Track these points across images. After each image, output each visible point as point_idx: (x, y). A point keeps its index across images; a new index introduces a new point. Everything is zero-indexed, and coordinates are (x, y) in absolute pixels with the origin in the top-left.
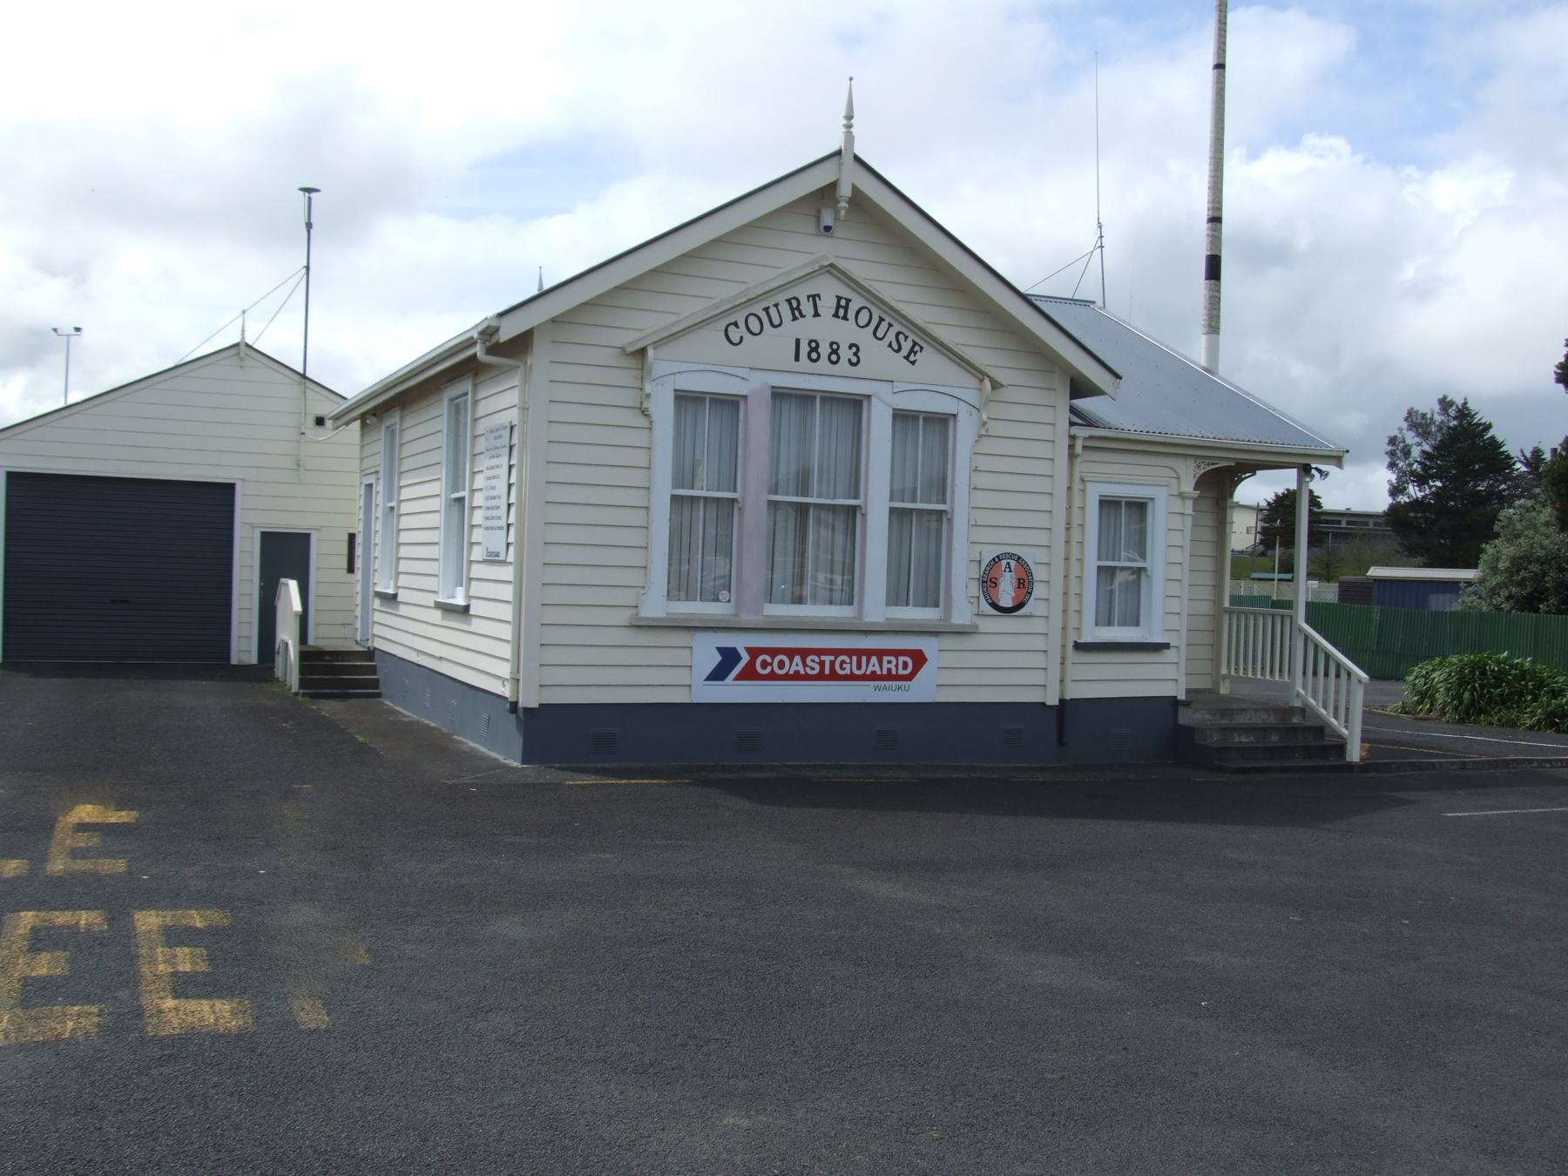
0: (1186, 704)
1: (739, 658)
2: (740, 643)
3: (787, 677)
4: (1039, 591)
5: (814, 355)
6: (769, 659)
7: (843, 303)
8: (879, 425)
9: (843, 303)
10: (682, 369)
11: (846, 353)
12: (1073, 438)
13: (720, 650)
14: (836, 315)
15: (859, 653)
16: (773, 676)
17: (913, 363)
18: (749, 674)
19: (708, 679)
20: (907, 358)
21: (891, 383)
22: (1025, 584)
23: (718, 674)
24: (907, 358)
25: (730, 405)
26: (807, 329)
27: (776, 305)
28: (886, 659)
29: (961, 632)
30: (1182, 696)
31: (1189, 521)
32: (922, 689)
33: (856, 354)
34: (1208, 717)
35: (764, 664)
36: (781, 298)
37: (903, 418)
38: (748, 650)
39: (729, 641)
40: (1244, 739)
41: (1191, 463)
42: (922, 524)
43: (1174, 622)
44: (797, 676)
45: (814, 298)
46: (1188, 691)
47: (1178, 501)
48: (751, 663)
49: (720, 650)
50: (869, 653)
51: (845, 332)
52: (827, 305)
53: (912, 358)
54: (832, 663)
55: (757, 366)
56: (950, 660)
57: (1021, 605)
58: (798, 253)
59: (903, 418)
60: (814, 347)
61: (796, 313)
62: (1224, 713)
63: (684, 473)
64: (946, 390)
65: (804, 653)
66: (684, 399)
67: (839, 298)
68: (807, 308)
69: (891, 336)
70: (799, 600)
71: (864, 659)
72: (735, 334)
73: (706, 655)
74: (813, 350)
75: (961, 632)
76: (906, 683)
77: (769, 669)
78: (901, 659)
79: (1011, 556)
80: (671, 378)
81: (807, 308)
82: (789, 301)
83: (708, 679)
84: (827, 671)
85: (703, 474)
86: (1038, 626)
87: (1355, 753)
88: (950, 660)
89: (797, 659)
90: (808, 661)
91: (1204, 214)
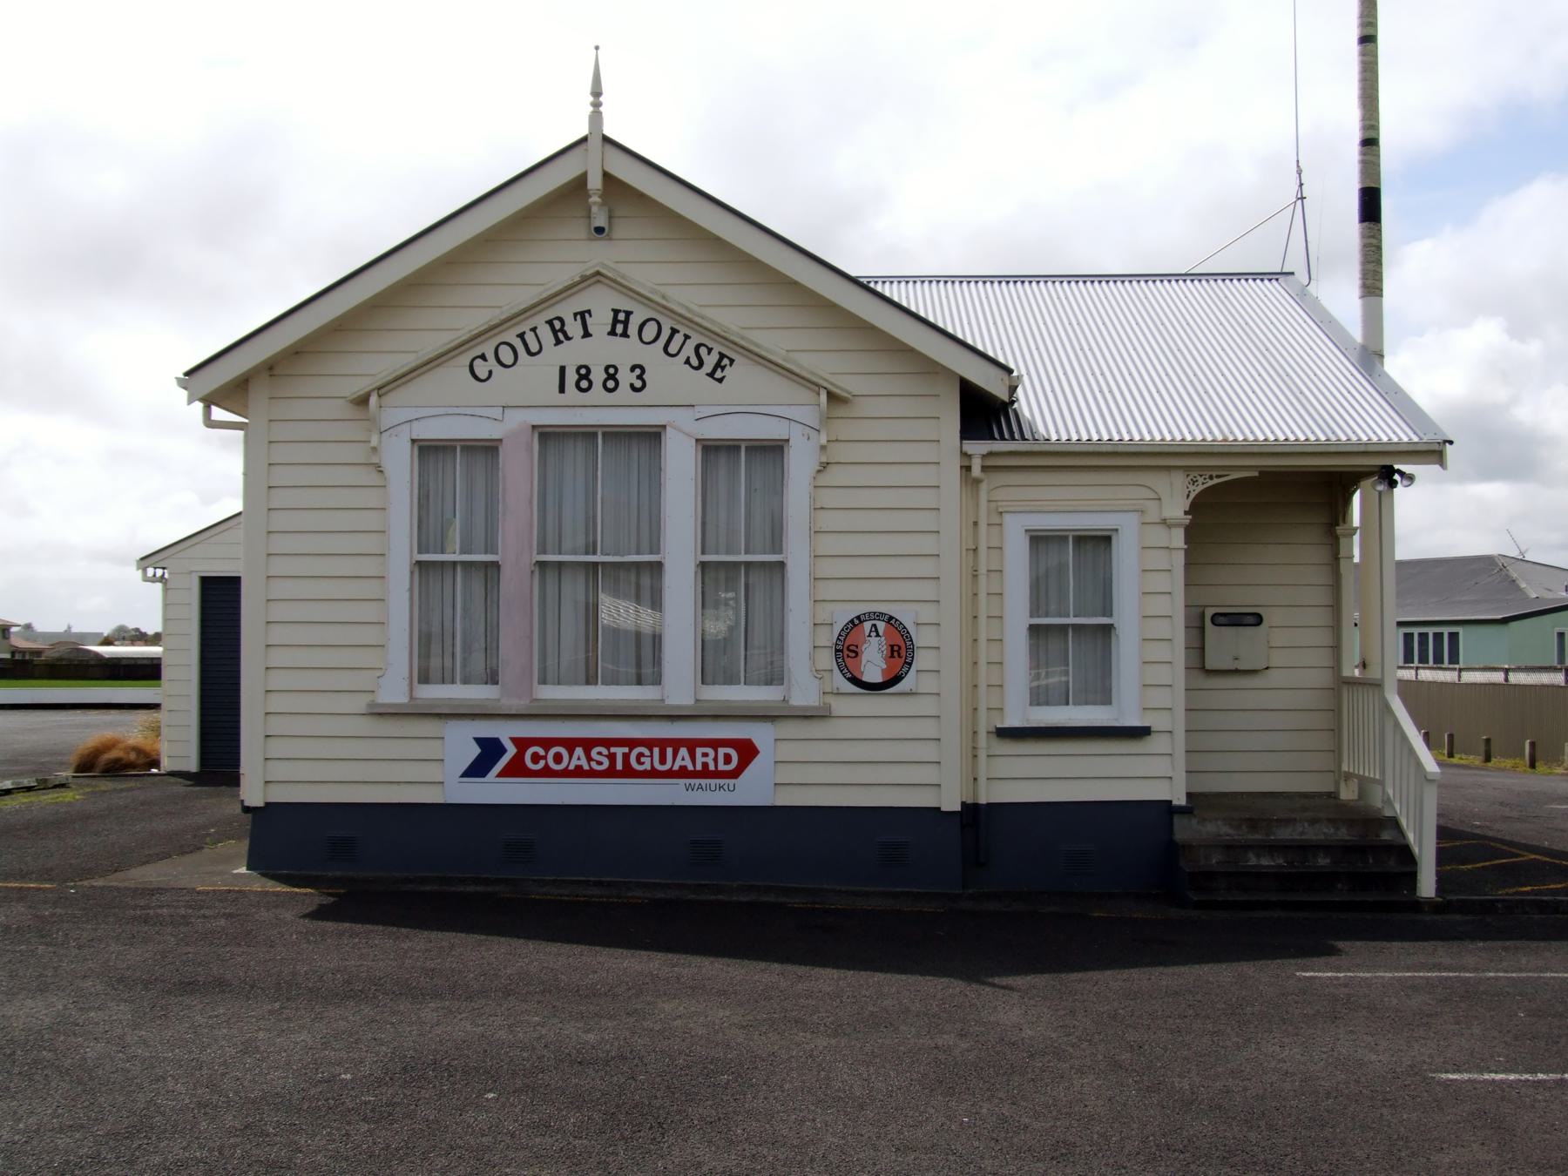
0: (1181, 810)
1: (503, 751)
2: (505, 732)
3: (566, 773)
4: (922, 660)
5: (584, 384)
6: (541, 752)
7: (621, 317)
8: (680, 463)
9: (621, 317)
10: (453, 409)
11: (626, 377)
12: (965, 455)
13: (479, 741)
14: (613, 333)
15: (663, 744)
16: (547, 772)
17: (720, 380)
18: (516, 769)
19: (463, 775)
20: (711, 375)
21: (688, 409)
22: (901, 652)
23: (477, 769)
24: (711, 375)
25: (488, 450)
26: (574, 353)
27: (534, 330)
28: (699, 751)
29: (807, 716)
30: (1180, 800)
31: (1179, 559)
32: (753, 789)
33: (640, 377)
34: (1225, 830)
35: (536, 758)
36: (540, 321)
37: (712, 450)
38: (514, 740)
39: (488, 730)
40: (1265, 862)
41: (1179, 480)
42: (743, 579)
43: (1160, 698)
44: (579, 772)
45: (582, 315)
46: (1189, 795)
47: (1161, 529)
48: (519, 758)
49: (479, 741)
50: (676, 744)
51: (625, 352)
52: (600, 321)
53: (718, 374)
54: (626, 757)
55: (514, 403)
56: (788, 751)
57: (896, 679)
58: (559, 260)
59: (712, 450)
60: (584, 374)
61: (560, 334)
62: (1253, 824)
63: (428, 531)
64: (469, 411)
65: (588, 744)
66: (428, 451)
67: (616, 312)
68: (574, 328)
69: (689, 350)
70: (590, 680)
71: (669, 751)
72: (481, 369)
73: (461, 744)
74: (582, 377)
75: (807, 716)
76: (731, 782)
77: (542, 763)
78: (722, 751)
79: (879, 616)
80: (406, 427)
81: (574, 328)
82: (550, 323)
83: (463, 775)
84: (619, 766)
85: (455, 536)
86: (925, 706)
87: (1427, 886)
88: (788, 751)
89: (579, 751)
90: (594, 753)
91: (1356, 136)
